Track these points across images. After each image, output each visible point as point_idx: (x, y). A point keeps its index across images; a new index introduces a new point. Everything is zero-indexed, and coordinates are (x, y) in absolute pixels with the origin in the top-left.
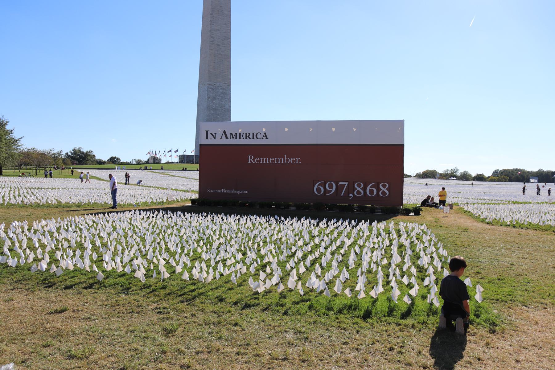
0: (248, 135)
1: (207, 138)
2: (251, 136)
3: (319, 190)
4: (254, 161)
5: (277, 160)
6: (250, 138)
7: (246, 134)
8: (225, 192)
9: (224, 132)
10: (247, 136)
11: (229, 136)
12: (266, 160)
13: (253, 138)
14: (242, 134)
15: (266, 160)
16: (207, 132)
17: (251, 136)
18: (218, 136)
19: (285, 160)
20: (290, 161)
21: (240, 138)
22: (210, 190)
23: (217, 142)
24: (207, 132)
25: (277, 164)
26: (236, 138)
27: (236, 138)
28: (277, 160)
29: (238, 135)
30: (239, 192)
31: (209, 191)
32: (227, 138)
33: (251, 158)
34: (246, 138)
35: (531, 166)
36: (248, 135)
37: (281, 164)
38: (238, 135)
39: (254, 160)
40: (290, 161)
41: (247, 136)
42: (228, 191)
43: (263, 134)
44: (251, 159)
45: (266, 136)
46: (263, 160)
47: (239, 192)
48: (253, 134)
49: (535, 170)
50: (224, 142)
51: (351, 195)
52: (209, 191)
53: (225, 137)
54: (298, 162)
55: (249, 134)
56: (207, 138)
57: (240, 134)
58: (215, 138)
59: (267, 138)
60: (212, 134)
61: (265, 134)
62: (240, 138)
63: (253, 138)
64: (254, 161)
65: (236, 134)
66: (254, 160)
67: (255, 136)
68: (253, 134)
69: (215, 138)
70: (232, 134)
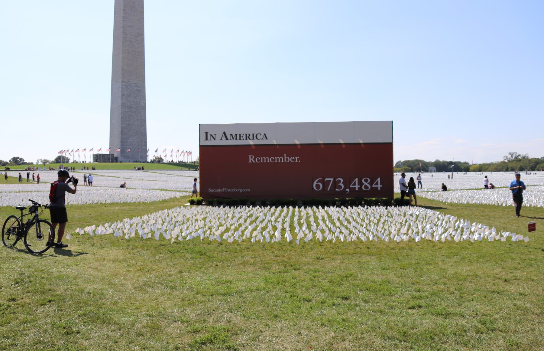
0: (248, 135)
1: (207, 139)
2: (251, 137)
3: (318, 186)
4: (255, 160)
5: (278, 159)
6: (250, 139)
7: (246, 135)
8: (227, 190)
9: (224, 133)
10: (247, 137)
11: (229, 137)
12: (267, 159)
13: (253, 139)
14: (241, 135)
15: (267, 159)
16: (207, 133)
17: (251, 137)
18: (218, 138)
19: (285, 159)
20: (290, 159)
21: (240, 139)
22: (212, 189)
23: (217, 142)
24: (207, 133)
25: (278, 163)
26: (236, 139)
27: (236, 139)
28: (278, 159)
29: (238, 136)
30: (241, 191)
31: (210, 190)
32: (227, 139)
33: (252, 157)
34: (246, 139)
35: (430, 158)
36: (248, 135)
37: (281, 163)
38: (238, 136)
39: (254, 160)
40: (290, 159)
41: (247, 137)
42: (230, 190)
43: (263, 135)
44: (251, 159)
45: (266, 137)
46: (263, 159)
47: (241, 191)
48: (253, 135)
49: (433, 160)
50: (224, 142)
51: (348, 190)
52: (210, 190)
53: (225, 138)
54: (298, 160)
55: (249, 135)
56: (207, 139)
57: (240, 135)
58: (215, 139)
59: (267, 139)
60: (211, 135)
61: (265, 134)
62: (240, 139)
63: (253, 139)
64: (255, 160)
65: (236, 135)
66: (254, 160)
67: (255, 137)
68: (253, 135)
69: (215, 139)
70: (232, 135)
